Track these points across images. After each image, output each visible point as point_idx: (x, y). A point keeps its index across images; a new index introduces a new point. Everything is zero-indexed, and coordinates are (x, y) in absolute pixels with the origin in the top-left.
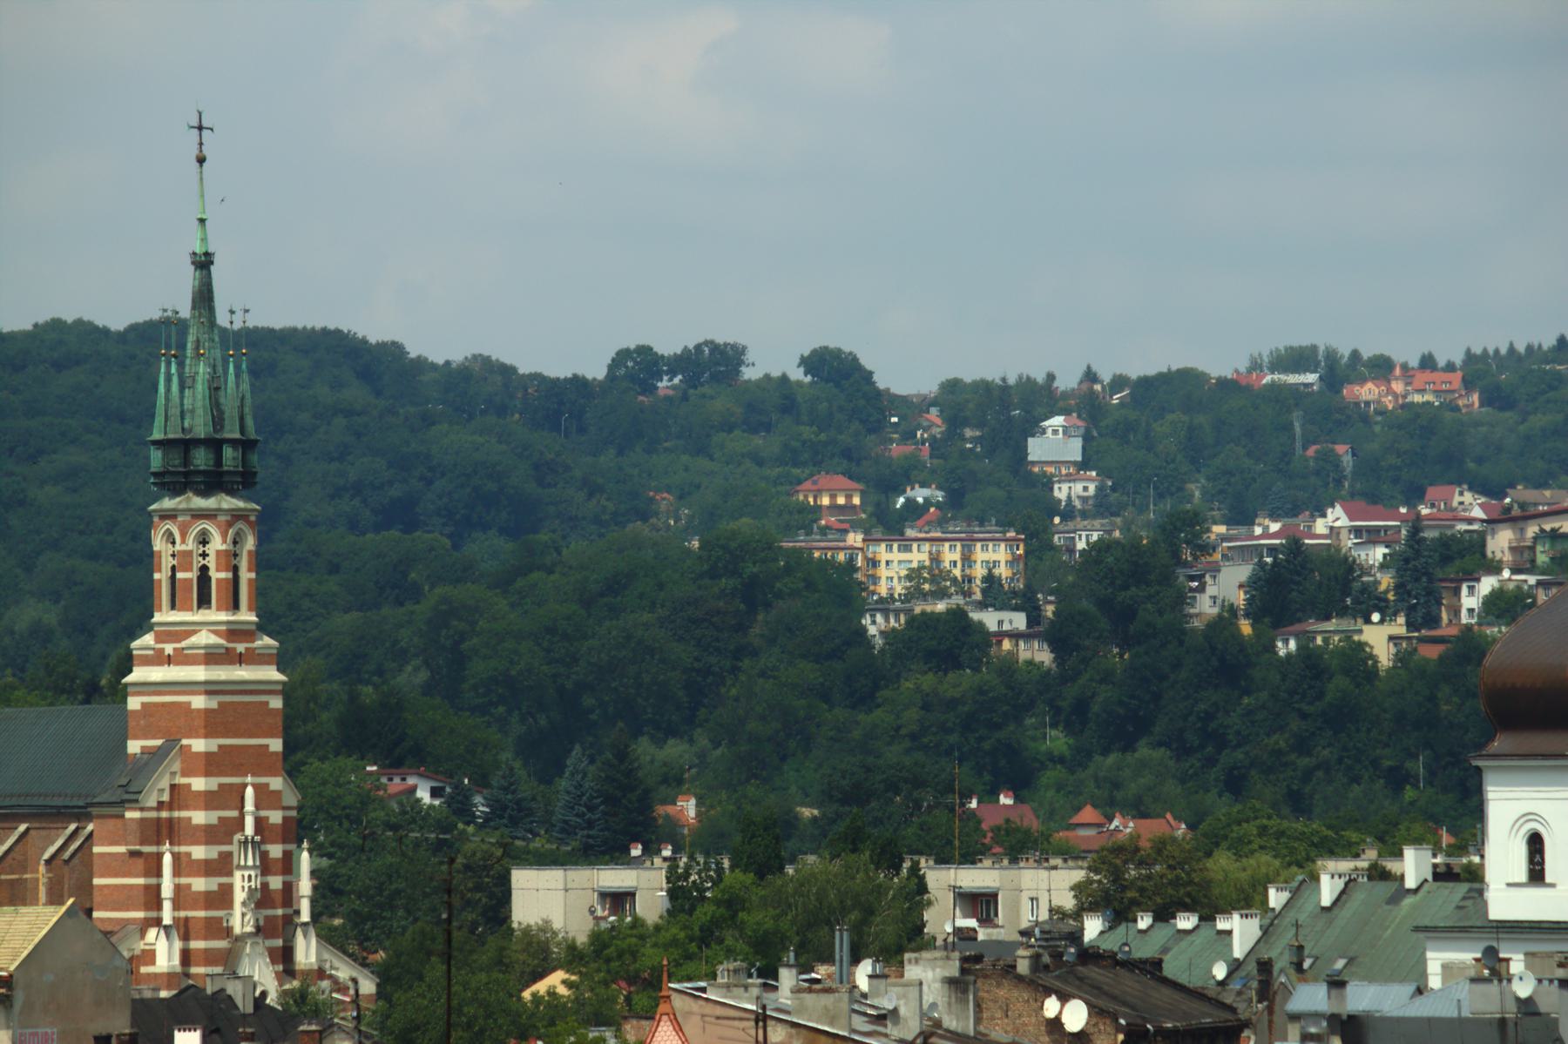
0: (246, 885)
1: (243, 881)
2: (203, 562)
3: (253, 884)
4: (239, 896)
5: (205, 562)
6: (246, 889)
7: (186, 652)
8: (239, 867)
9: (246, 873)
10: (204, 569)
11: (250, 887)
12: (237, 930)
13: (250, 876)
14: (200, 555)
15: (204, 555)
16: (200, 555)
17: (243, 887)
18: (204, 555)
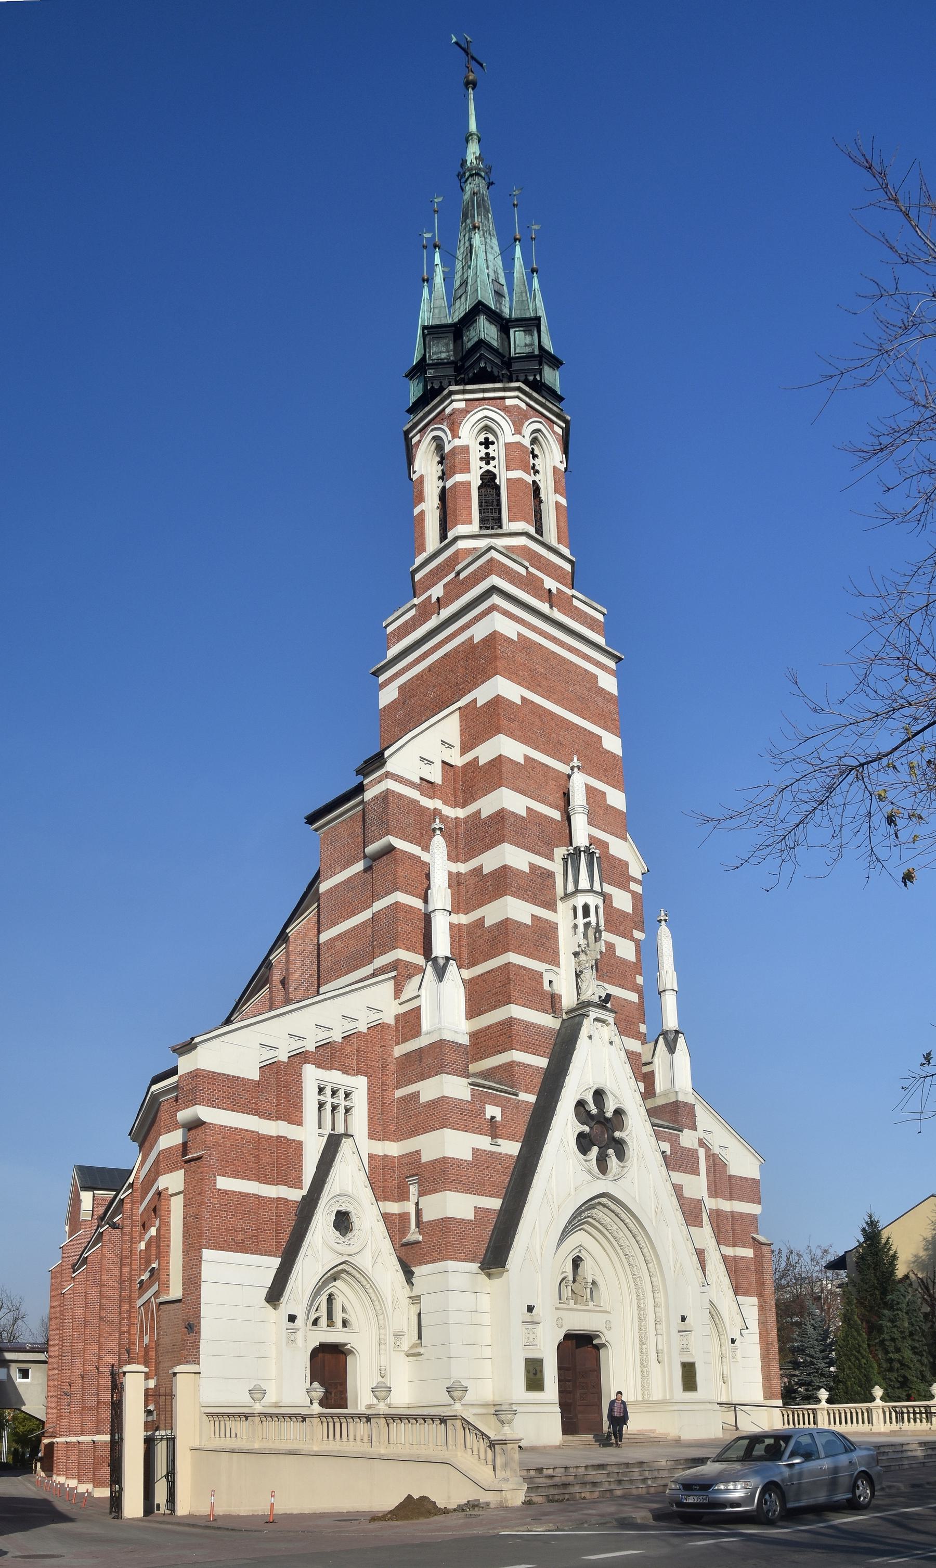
0: (581, 921)
1: (575, 917)
2: (486, 468)
3: (592, 919)
4: (567, 942)
5: (490, 467)
6: (581, 928)
7: (462, 576)
8: (566, 896)
9: (580, 900)
10: (489, 480)
11: (587, 925)
12: (568, 1000)
13: (586, 908)
14: (481, 459)
15: (487, 459)
16: (481, 459)
17: (575, 926)
18: (487, 459)
